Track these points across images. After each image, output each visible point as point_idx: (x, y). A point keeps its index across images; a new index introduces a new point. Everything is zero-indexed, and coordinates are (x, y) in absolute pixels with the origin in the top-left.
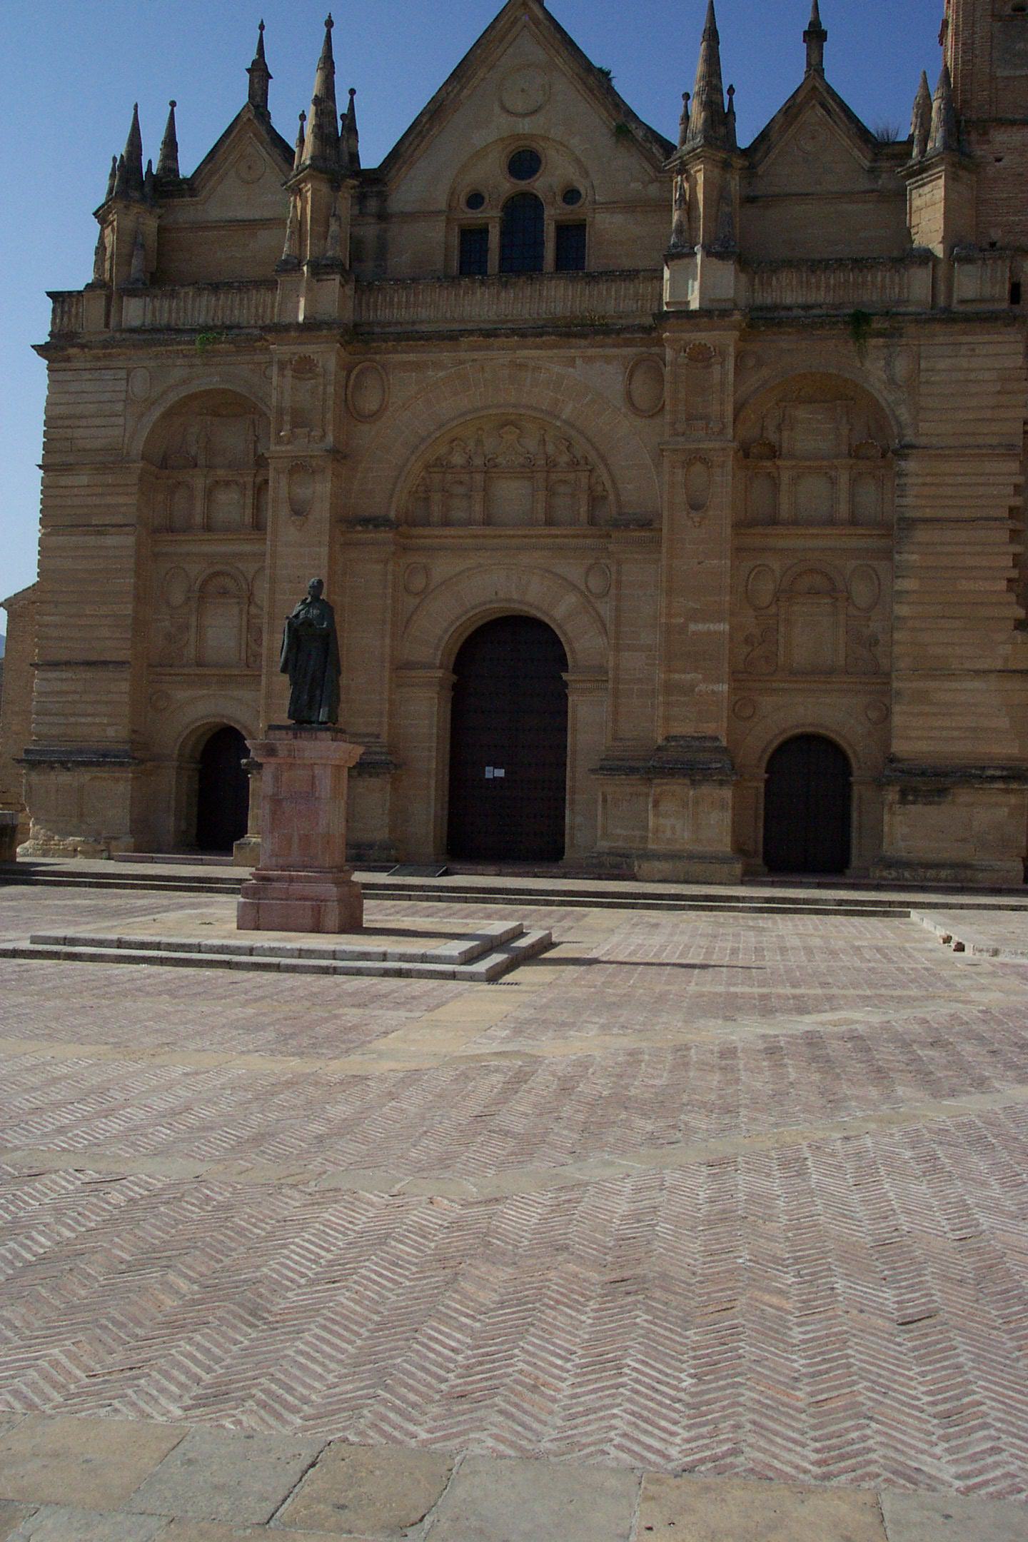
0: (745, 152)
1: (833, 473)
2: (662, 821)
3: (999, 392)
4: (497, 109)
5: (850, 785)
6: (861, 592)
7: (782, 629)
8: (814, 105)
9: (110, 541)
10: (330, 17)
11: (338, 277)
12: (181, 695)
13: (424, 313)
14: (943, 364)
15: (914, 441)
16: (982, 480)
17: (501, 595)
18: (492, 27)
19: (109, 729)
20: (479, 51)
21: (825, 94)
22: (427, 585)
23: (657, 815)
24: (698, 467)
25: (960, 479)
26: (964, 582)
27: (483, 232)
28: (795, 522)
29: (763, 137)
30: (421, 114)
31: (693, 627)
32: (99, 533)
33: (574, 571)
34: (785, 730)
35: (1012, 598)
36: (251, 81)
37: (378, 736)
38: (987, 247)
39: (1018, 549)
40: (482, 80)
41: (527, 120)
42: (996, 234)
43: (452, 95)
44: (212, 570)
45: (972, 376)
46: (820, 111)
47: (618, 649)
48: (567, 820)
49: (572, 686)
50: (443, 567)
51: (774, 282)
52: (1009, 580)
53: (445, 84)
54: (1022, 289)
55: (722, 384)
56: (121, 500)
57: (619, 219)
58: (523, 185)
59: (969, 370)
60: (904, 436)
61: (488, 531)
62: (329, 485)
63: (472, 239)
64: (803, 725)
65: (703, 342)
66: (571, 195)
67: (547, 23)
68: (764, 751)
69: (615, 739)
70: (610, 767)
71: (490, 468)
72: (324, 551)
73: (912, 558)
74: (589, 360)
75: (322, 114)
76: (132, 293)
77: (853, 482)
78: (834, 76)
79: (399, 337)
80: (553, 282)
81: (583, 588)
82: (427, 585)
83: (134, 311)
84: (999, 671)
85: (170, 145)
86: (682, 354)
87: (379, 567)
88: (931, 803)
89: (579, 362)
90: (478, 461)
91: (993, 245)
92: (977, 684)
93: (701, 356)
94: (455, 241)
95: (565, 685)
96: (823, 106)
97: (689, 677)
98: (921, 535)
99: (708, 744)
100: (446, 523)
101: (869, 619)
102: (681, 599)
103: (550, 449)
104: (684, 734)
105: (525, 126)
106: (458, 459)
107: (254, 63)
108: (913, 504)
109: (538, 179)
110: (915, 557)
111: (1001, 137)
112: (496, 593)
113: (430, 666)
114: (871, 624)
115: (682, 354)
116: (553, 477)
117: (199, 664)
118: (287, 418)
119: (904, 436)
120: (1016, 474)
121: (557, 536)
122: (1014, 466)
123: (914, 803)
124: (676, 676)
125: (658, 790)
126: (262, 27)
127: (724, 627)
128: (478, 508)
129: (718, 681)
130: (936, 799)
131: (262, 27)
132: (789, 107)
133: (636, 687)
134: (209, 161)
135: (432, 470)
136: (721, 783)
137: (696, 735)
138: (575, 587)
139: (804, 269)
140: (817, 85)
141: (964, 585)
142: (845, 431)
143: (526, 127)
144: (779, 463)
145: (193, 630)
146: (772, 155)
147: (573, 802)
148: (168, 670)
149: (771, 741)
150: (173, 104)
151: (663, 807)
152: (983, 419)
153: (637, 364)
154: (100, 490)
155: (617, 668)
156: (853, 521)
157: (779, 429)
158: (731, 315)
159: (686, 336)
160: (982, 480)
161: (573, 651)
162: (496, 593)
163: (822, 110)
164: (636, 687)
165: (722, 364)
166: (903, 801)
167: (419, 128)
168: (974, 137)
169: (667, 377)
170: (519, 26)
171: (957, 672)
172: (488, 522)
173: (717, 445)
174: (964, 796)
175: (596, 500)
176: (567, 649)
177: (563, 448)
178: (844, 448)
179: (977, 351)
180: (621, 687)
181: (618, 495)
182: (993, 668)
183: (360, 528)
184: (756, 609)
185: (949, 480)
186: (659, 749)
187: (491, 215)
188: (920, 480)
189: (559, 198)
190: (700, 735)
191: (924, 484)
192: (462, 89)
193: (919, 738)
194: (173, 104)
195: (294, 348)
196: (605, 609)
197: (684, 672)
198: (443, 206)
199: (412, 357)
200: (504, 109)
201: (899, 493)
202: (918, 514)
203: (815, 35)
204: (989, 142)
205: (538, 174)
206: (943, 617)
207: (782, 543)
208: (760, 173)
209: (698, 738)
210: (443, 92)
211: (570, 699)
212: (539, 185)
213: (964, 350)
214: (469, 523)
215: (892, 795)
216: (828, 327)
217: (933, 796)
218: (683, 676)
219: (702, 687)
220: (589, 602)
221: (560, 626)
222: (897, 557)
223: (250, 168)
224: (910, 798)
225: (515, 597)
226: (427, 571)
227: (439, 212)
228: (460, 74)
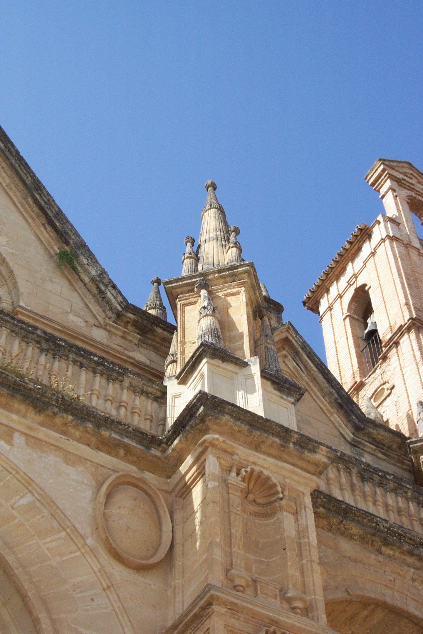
8: (285, 356)
21: (300, 350)
65: (266, 473)
86: (234, 474)
89: (19, 440)
139: (355, 470)
140: (291, 338)
158: (313, 451)
216: (406, 547)
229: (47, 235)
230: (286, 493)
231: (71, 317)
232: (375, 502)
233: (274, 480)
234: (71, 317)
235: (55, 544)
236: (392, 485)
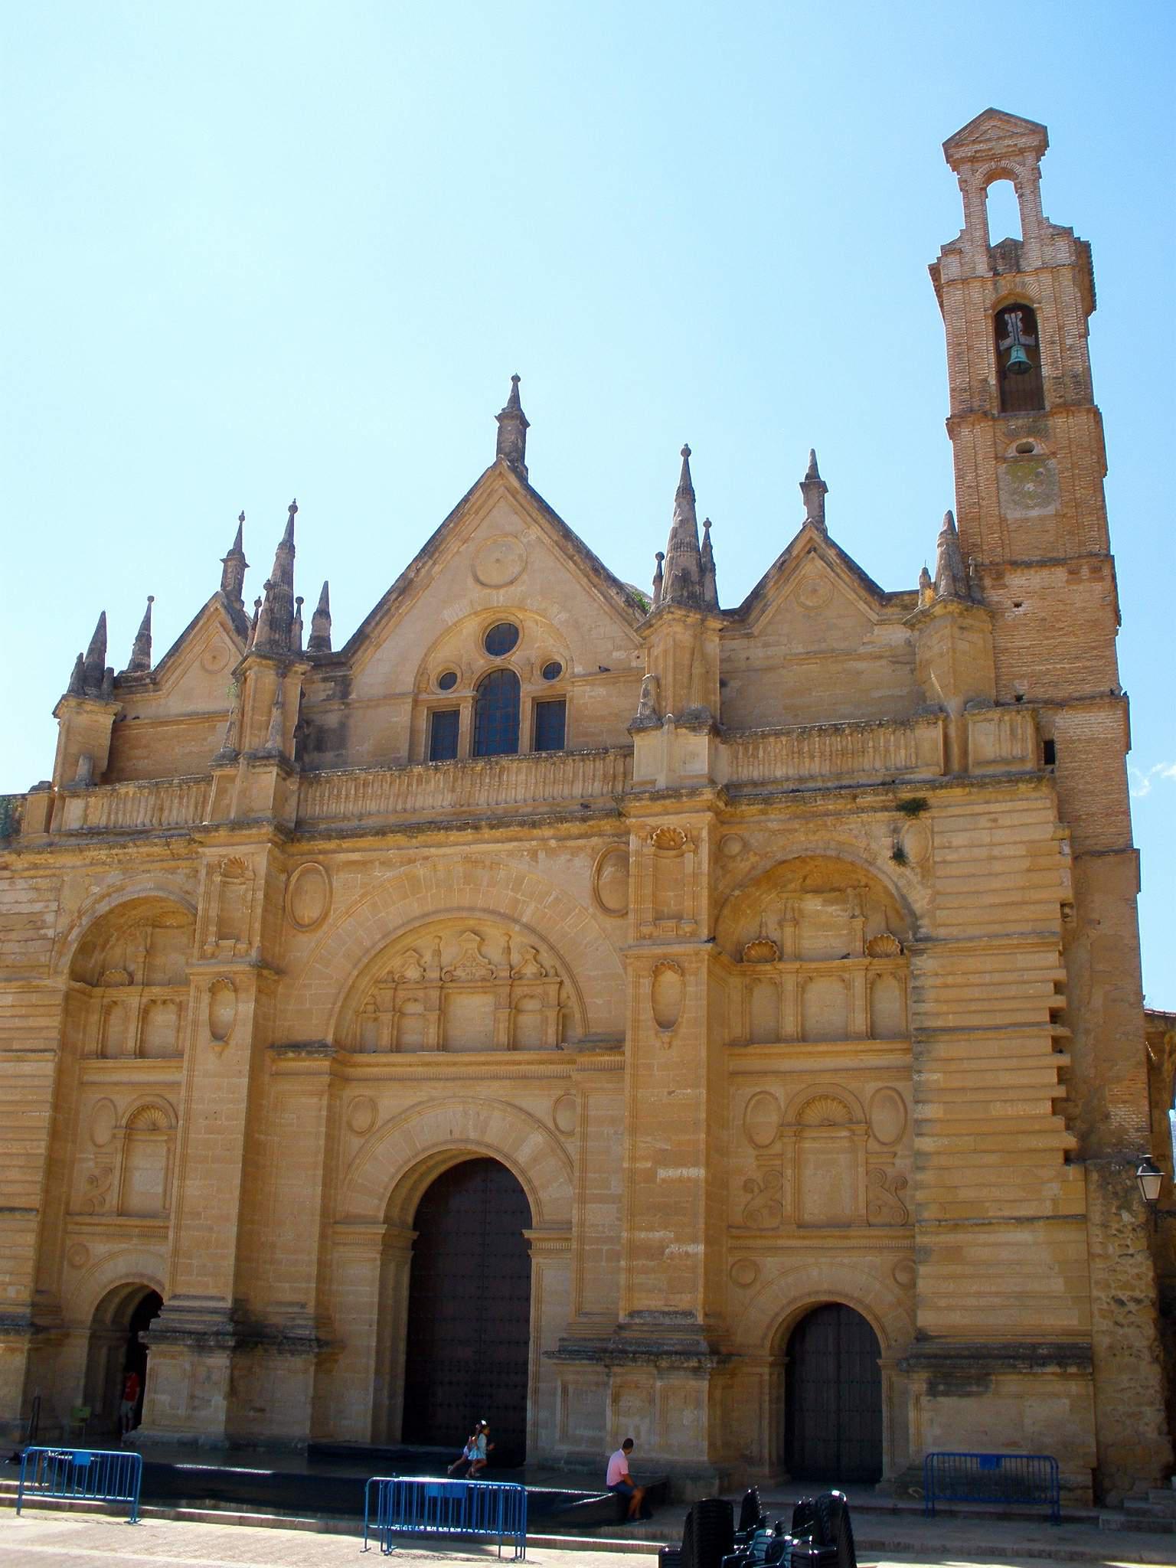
0: (741, 616)
1: (846, 976)
2: (623, 1420)
3: (1029, 870)
4: (470, 581)
5: (877, 1370)
6: (885, 1122)
7: (789, 1172)
8: (813, 558)
9: (27, 1068)
10: (294, 502)
11: (275, 770)
12: (100, 1248)
13: (372, 806)
14: (959, 840)
15: (934, 933)
16: (1010, 977)
17: (457, 1135)
18: (465, 500)
19: (10, 1288)
20: (451, 525)
22: (373, 1124)
23: (617, 1413)
24: (669, 977)
25: (987, 978)
26: (998, 1104)
27: (456, 714)
28: (803, 1038)
29: (757, 594)
30: (389, 593)
31: (663, 1173)
32: (20, 1060)
33: (539, 1103)
34: (795, 1299)
35: (1059, 1122)
36: (225, 572)
37: (303, 1306)
38: (1013, 701)
39: (1064, 1060)
40: (458, 552)
41: (502, 591)
42: (1022, 687)
43: (423, 571)
44: (137, 1104)
45: (996, 852)
46: (820, 563)
47: (582, 1200)
48: (529, 1415)
49: (536, 1245)
50: (391, 1101)
51: (761, 754)
52: (1054, 1100)
53: (415, 560)
54: (1057, 746)
55: (695, 875)
56: (43, 1022)
57: (601, 691)
58: (498, 661)
59: (992, 845)
60: (919, 927)
61: (442, 1057)
62: (252, 1005)
63: (443, 722)
64: (817, 1293)
66: (552, 671)
67: (523, 492)
68: (769, 1327)
69: (580, 1312)
70: (570, 1351)
71: (447, 981)
72: (245, 1081)
73: (933, 1077)
74: (551, 853)
75: (274, 598)
76: (75, 795)
77: (871, 986)
78: (837, 529)
79: (342, 835)
80: (515, 764)
81: (551, 1125)
82: (373, 1124)
84: (1048, 1218)
85: (144, 639)
86: (649, 841)
87: (315, 1100)
88: (969, 1394)
89: (542, 855)
90: (434, 974)
91: (1019, 699)
92: (1023, 1235)
93: (666, 842)
94: (423, 724)
95: (528, 1243)
96: (822, 558)
97: (658, 1235)
98: (942, 1048)
99: (680, 1321)
100: (397, 1048)
101: (895, 1154)
102: (649, 1139)
103: (515, 958)
104: (653, 1308)
105: (500, 598)
106: (413, 973)
107: (230, 553)
108: (935, 1010)
109: (515, 653)
110: (935, 1077)
111: (1017, 580)
112: (451, 1131)
113: (374, 1222)
114: (897, 1161)
115: (649, 841)
116: (519, 991)
117: (122, 1213)
118: (213, 929)
119: (919, 927)
120: (1056, 968)
121: (519, 1063)
122: (1053, 958)
123: (946, 1394)
124: (643, 1235)
125: (618, 1380)
126: (242, 518)
127: (699, 1173)
128: (433, 1030)
129: (694, 1240)
130: (974, 1388)
131: (242, 518)
132: (782, 564)
133: (605, 1248)
134: (173, 655)
135: (382, 986)
136: (696, 1371)
137: (666, 1309)
138: (540, 1124)
140: (814, 536)
141: (998, 1110)
142: (858, 923)
143: (501, 598)
144: (781, 966)
145: (117, 1173)
146: (770, 611)
147: (536, 1391)
148: (88, 1220)
149: (777, 1314)
150: (151, 599)
151: (623, 1404)
152: (1013, 904)
153: (604, 856)
154: (23, 1011)
155: (582, 1224)
156: (872, 1034)
157: (780, 924)
158: (701, 794)
159: (652, 821)
160: (1010, 977)
161: (538, 1203)
162: (451, 1131)
163: (822, 563)
164: (605, 1248)
165: (695, 852)
166: (932, 1391)
167: (386, 607)
168: (987, 582)
169: (632, 870)
170: (496, 497)
171: (994, 1221)
172: (444, 1046)
173: (689, 948)
174: (1010, 1383)
175: (564, 1020)
176: (530, 1199)
177: (529, 957)
178: (858, 946)
179: (1001, 822)
180: (587, 1248)
181: (584, 1011)
182: (1040, 1214)
183: (291, 1055)
184: (758, 1147)
185: (974, 979)
186: (621, 1327)
187: (463, 697)
188: (939, 981)
189: (537, 673)
190: (671, 1309)
191: (946, 986)
192: (434, 564)
193: (950, 1308)
194: (151, 599)
195: (223, 851)
196: (572, 1146)
197: (651, 1229)
198: (410, 688)
199: (355, 856)
200: (477, 580)
201: (915, 999)
202: (939, 1023)
203: (814, 486)
204: (1005, 586)
205: (515, 649)
206: (975, 1151)
207: (786, 1065)
208: (756, 634)
209: (668, 1313)
210: (414, 568)
211: (534, 1262)
212: (515, 660)
213: (984, 822)
214: (423, 1048)
215: (918, 1383)
217: (970, 1384)
218: (651, 1235)
219: (674, 1248)
220: (558, 1142)
221: (523, 1172)
222: (916, 1077)
223: (214, 657)
224: (941, 1388)
225: (473, 1135)
226: (373, 1105)
227: (403, 695)
228: (432, 549)
229: (585, 580)
230: (689, 836)
231: (616, 654)
232: (812, 757)
233: (679, 830)
234: (616, 654)
235: (572, 921)
236: (830, 731)
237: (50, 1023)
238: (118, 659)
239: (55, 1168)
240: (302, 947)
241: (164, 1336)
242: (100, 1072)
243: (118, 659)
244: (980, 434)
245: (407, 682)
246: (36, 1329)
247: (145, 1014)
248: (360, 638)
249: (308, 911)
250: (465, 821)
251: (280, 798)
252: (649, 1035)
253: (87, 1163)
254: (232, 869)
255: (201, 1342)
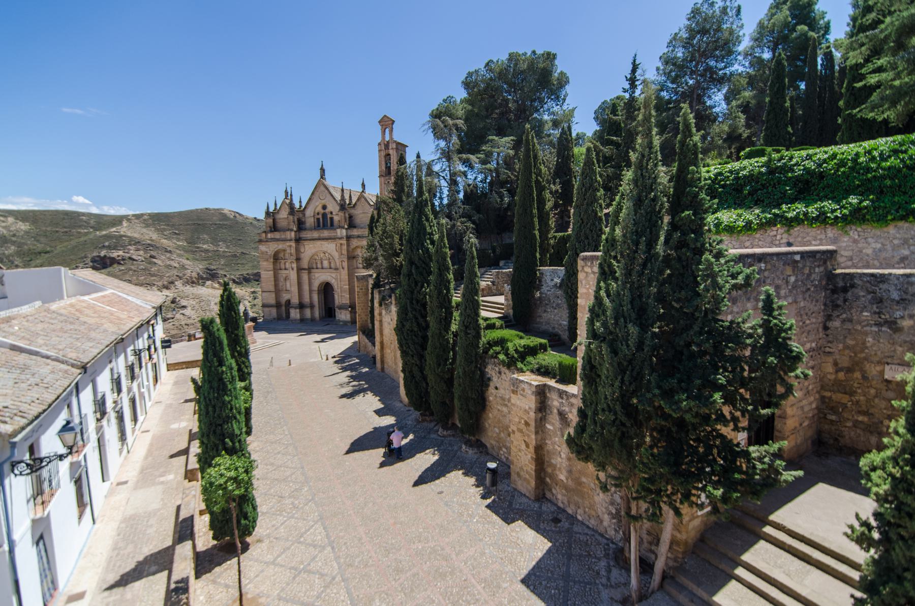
33: (334, 275)
50: (317, 275)
83: (269, 236)
85: (276, 204)
105: (323, 202)
187: (320, 216)
228: (313, 193)
237: (271, 266)
238: (271, 210)
239: (276, 285)
240: (302, 256)
241: (292, 307)
242: (280, 272)
243: (271, 210)
244: (383, 178)
245: (312, 215)
246: (277, 307)
247: (285, 263)
248: (305, 207)
249: (302, 250)
250: (319, 239)
251: (295, 235)
252: (342, 270)
253: (281, 284)
254: (290, 246)
255: (295, 308)
